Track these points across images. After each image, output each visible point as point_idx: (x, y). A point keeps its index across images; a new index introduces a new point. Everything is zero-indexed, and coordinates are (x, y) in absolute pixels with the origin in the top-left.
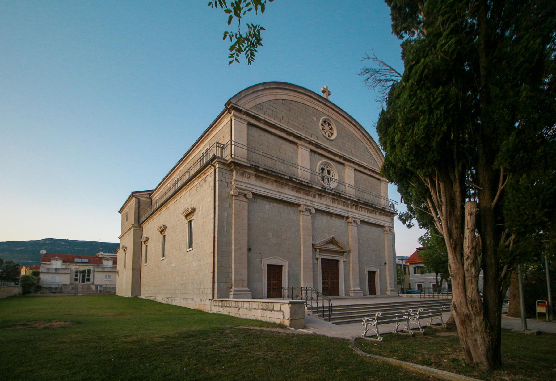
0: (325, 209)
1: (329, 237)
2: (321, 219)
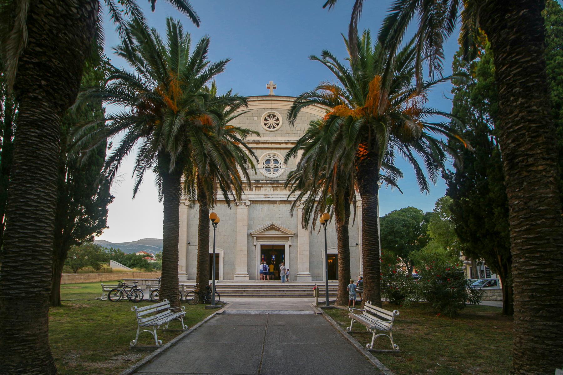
0: (264, 199)
1: (268, 223)
2: (262, 209)
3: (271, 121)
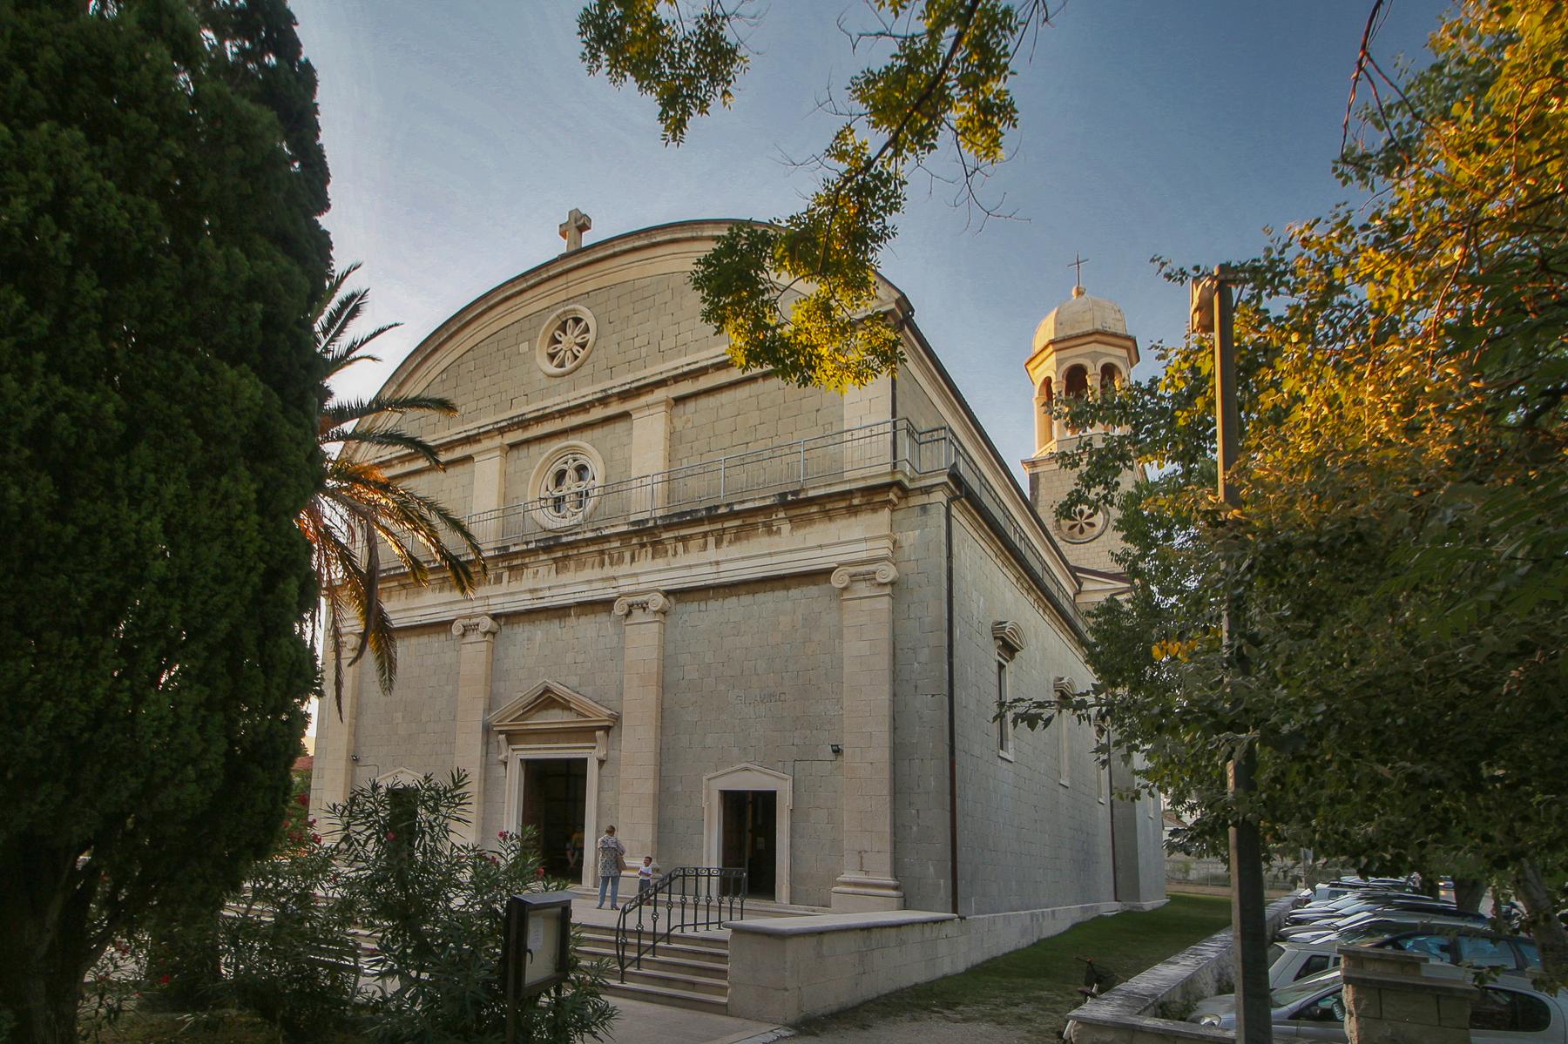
0: (528, 605)
3: (569, 340)
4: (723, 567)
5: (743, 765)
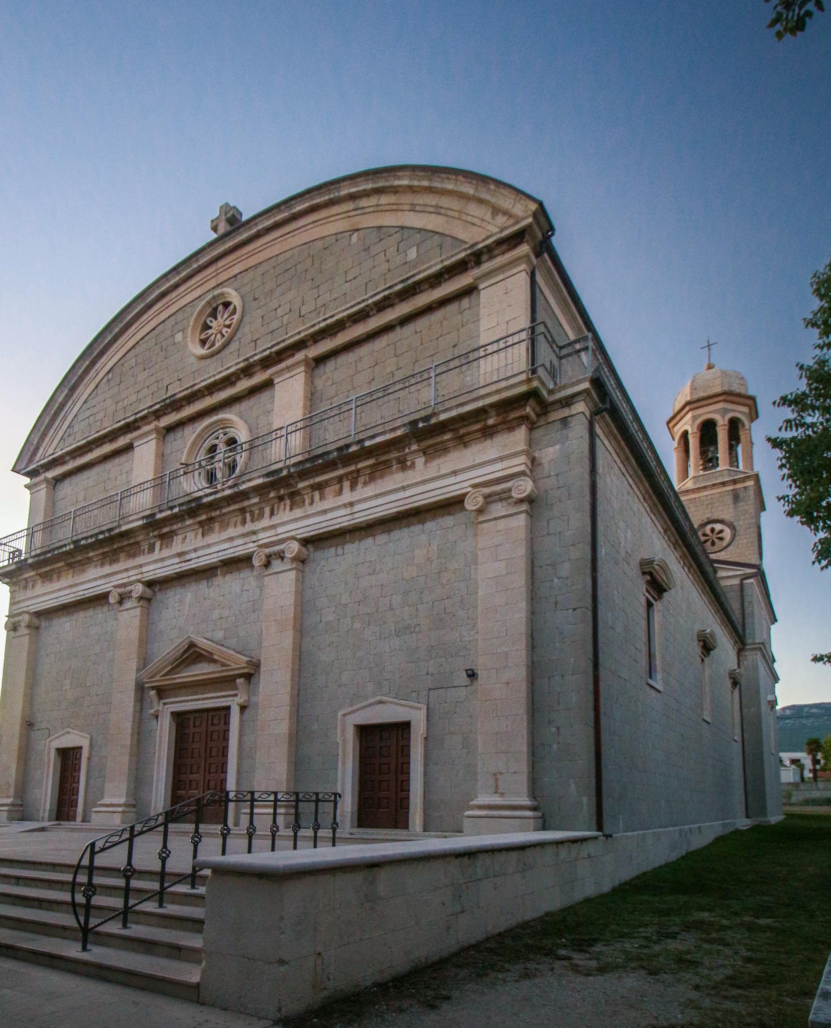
4: (357, 508)
5: (379, 698)
